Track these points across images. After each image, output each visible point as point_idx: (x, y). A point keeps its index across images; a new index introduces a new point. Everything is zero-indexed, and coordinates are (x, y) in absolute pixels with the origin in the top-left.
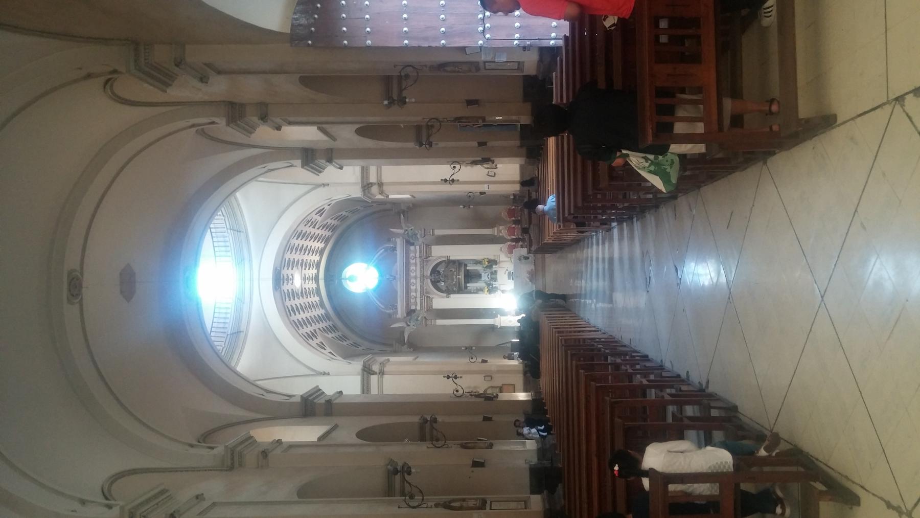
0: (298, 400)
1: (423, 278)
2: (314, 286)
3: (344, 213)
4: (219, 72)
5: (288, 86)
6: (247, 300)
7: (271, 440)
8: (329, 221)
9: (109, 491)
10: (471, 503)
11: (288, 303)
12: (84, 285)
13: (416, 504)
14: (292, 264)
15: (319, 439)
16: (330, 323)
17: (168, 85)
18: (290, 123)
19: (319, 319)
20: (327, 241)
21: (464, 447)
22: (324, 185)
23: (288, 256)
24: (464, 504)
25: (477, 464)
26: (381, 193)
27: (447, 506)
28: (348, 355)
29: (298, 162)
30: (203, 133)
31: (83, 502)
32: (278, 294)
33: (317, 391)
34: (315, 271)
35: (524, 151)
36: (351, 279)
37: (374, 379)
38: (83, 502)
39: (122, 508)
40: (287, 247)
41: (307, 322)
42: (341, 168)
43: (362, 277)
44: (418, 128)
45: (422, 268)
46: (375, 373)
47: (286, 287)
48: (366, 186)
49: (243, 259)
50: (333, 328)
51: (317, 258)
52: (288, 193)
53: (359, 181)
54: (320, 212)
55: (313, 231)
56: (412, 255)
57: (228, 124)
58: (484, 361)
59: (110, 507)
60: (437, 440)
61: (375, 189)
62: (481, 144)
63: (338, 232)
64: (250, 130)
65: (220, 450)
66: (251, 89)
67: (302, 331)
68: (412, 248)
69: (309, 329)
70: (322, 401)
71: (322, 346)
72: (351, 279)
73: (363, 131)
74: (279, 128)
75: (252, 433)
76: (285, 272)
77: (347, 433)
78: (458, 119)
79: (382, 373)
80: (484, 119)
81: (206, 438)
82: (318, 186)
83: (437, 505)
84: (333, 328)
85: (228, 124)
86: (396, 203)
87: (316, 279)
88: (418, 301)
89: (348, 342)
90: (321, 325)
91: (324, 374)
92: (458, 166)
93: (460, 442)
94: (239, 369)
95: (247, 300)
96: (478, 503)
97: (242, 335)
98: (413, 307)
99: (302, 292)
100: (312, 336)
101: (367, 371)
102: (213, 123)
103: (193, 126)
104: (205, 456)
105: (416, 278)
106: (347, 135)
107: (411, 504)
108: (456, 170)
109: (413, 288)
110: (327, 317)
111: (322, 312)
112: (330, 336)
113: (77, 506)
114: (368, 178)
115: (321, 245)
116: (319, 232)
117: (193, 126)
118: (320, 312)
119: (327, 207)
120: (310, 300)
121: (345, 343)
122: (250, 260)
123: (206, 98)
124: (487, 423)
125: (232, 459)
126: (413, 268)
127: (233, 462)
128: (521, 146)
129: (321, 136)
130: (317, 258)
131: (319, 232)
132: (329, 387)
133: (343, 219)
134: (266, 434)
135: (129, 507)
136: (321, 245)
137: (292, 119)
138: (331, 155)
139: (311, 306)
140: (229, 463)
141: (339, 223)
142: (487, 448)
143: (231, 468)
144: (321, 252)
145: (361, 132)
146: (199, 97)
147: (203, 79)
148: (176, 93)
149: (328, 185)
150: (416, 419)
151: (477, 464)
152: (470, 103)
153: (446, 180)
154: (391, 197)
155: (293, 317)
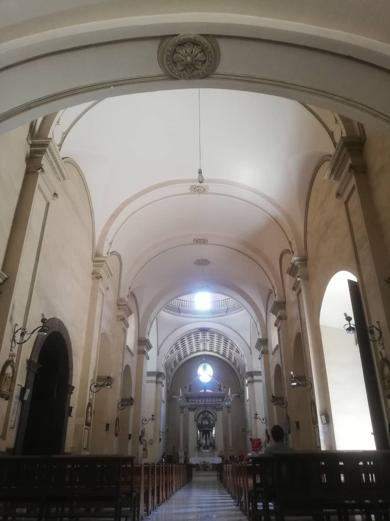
0: (147, 337)
1: (205, 406)
2: (201, 349)
3: (238, 364)
4: (298, 295)
5: (295, 328)
6: (195, 316)
7: (129, 323)
8: (233, 356)
9: (115, 254)
10: (89, 418)
11: (193, 335)
12: (202, 245)
13: (92, 388)
14: (212, 337)
15: (127, 346)
16: (183, 357)
17: (290, 274)
18: (279, 330)
19: (185, 351)
20: (224, 355)
21: (117, 420)
23: (216, 335)
24: (89, 414)
25: (108, 425)
26: (249, 382)
27: (90, 405)
28: (167, 366)
29: (261, 337)
30: (271, 292)
31: (111, 243)
32: (197, 330)
33: (150, 347)
34: (208, 349)
36: (205, 367)
37: (154, 378)
38: (111, 243)
39: (106, 257)
40: (220, 335)
41: (184, 345)
42: (260, 359)
43: (205, 374)
44: (282, 399)
45: (210, 405)
46: (157, 378)
48: (251, 374)
49: (213, 314)
50: (180, 359)
51: (215, 350)
53: (254, 370)
54: (238, 351)
55: (228, 348)
56: (217, 400)
57: (275, 302)
58: (160, 439)
59: (107, 253)
60: (122, 405)
64: (274, 312)
65: (127, 300)
66: (292, 312)
67: (179, 342)
68: (220, 400)
69: (180, 346)
70: (145, 349)
71: (172, 352)
72: (205, 367)
73: (278, 368)
74: (276, 325)
75: (133, 315)
76: (208, 334)
77: (131, 361)
78: (288, 418)
79: (157, 382)
80: (289, 432)
81: (132, 295)
82: (250, 349)
83: (90, 399)
84: (180, 359)
85: (275, 302)
86: (243, 392)
88: (193, 403)
89: (173, 366)
91: (158, 353)
92: (264, 422)
93: (119, 418)
94: (162, 312)
95: (195, 316)
96: (89, 421)
97: (178, 314)
98: (190, 400)
100: (177, 348)
101: (159, 375)
102: (275, 296)
103: (273, 287)
104: (124, 294)
105: (205, 402)
106: (275, 360)
107: (92, 386)
108: (262, 421)
109: (200, 401)
110: (186, 356)
111: (188, 353)
112: (177, 357)
113: (110, 241)
114: (256, 375)
115: (221, 352)
116: (228, 352)
117: (273, 287)
118: (188, 352)
119: (240, 354)
120: (194, 347)
121: (173, 364)
122: (213, 317)
123: (286, 292)
124: (128, 436)
125: (122, 305)
126: (210, 400)
127: (120, 304)
129: (274, 347)
130: (215, 350)
131: (228, 352)
132: (152, 353)
133: (235, 364)
134: (132, 320)
135: (107, 260)
136: (221, 353)
137: (280, 331)
138: (265, 353)
139: (191, 348)
141: (233, 361)
142: (115, 432)
143: (118, 305)
145: (278, 366)
146: (287, 289)
147: (294, 289)
148: (288, 278)
151: (108, 425)
152: (297, 424)
153: (256, 415)
155: (186, 338)
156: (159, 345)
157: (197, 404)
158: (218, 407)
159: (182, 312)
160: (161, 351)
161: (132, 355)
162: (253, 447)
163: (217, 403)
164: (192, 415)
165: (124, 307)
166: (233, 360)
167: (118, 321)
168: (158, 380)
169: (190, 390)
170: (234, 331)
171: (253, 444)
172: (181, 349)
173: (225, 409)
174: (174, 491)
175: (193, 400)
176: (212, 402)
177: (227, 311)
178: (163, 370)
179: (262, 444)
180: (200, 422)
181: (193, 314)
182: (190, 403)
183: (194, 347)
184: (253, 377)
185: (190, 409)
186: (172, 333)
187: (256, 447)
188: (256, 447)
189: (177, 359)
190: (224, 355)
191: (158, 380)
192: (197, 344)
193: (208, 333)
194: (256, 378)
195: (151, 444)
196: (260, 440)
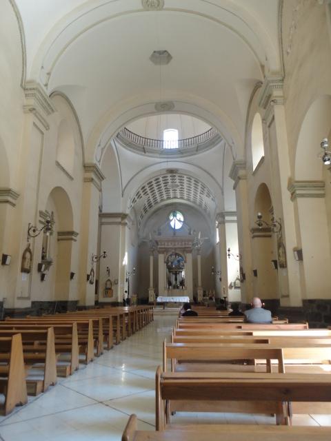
1: (175, 249)
2: (172, 196)
11: (161, 179)
19: (155, 199)
23: (185, 179)
26: (219, 223)
42: (234, 188)
47: (169, 175)
49: (182, 153)
50: (150, 206)
51: (186, 198)
61: (220, 219)
62: (255, 273)
63: (198, 208)
69: (148, 190)
87: (175, 198)
88: (163, 247)
89: (143, 213)
90: (152, 200)
97: (143, 153)
110: (156, 203)
115: (192, 200)
118: (159, 199)
122: (181, 157)
125: (30, 89)
130: (186, 198)
133: (205, 210)
139: (161, 195)
140: (27, 87)
144: (188, 200)
150: (76, 229)
154: (217, 229)
156: (124, 185)
158: (189, 249)
160: (125, 193)
161: (71, 178)
163: (187, 246)
164: (161, 258)
165: (33, 92)
166: (203, 206)
167: (25, 112)
169: (160, 234)
170: (205, 171)
172: (150, 194)
174: (138, 328)
177: (198, 149)
178: (128, 212)
180: (170, 264)
182: (159, 246)
183: (164, 193)
184: (224, 218)
185: (159, 252)
189: (147, 205)
190: (194, 202)
192: (167, 190)
193: (177, 175)
194: (227, 218)
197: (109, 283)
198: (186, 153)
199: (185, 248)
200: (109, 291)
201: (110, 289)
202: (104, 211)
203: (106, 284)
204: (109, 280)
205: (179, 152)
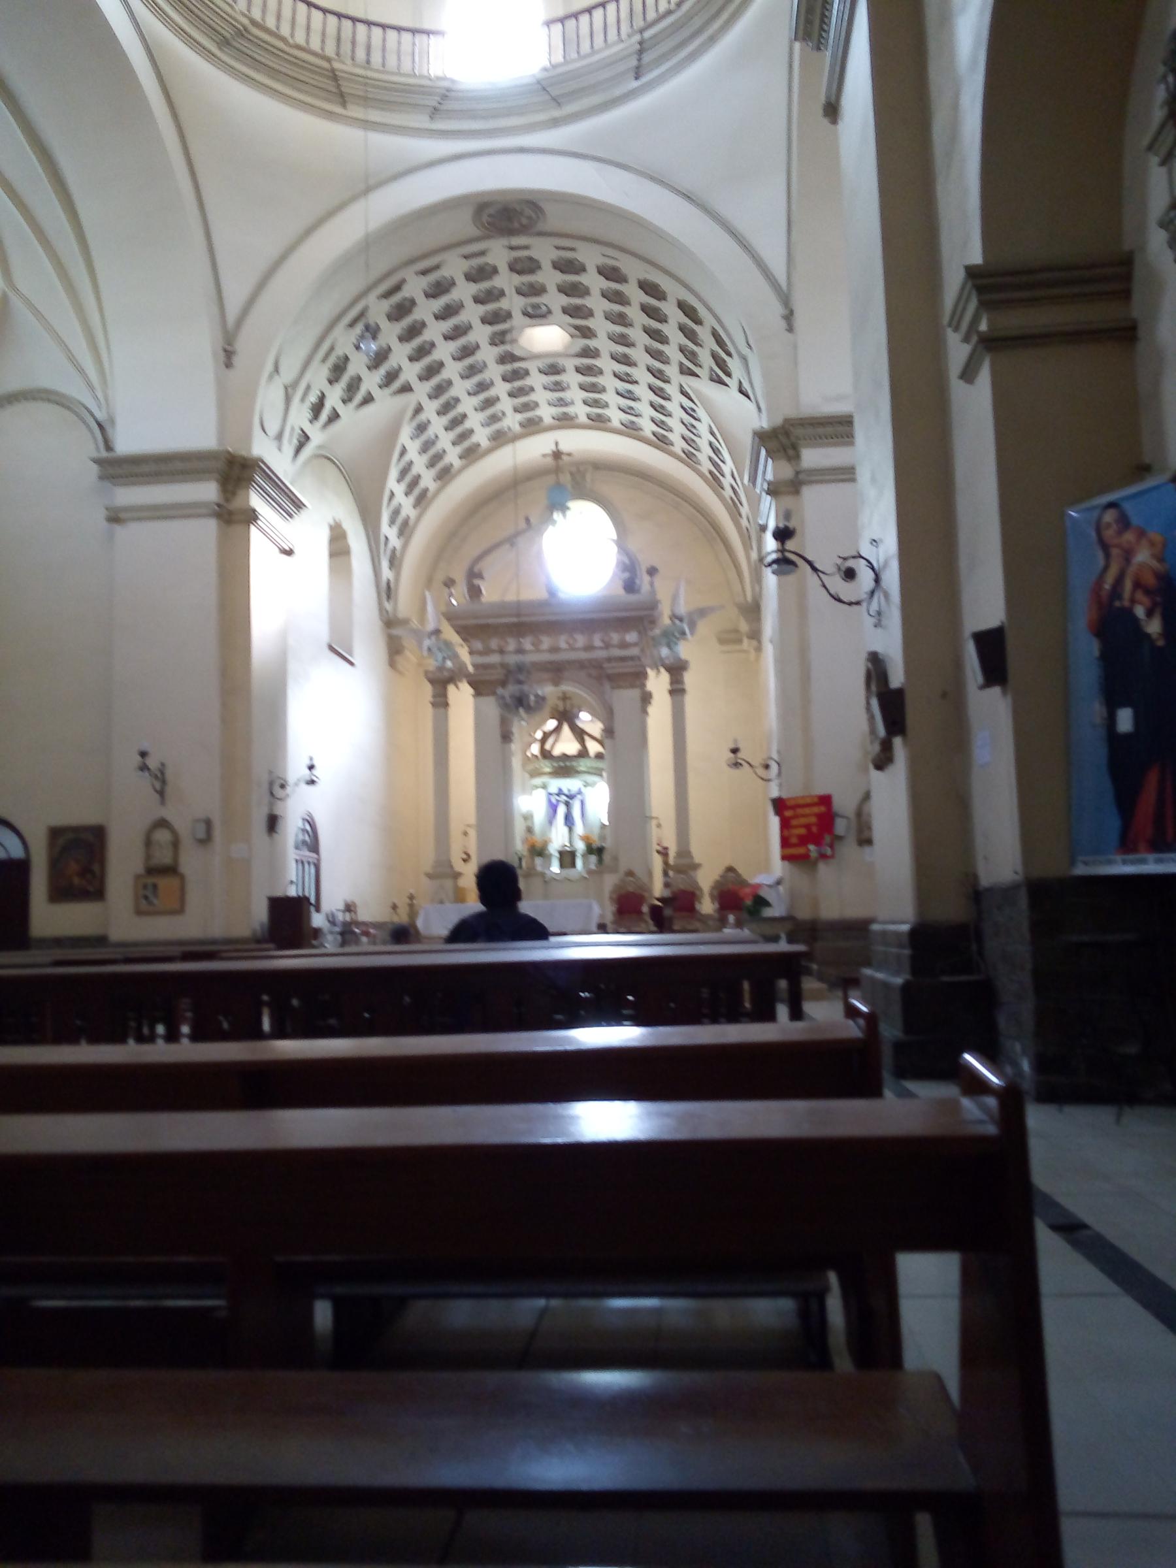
22: (789, 317)
35: (951, 909)
37: (208, 491)
45: (581, 665)
47: (498, 253)
49: (557, 101)
52: (761, 211)
56: (615, 637)
88: (494, 659)
91: (228, 356)
99: (513, 358)
108: (837, 584)
109: (527, 643)
122: (555, 123)
126: (581, 640)
128: (977, 895)
149: (790, 329)
156: (233, 309)
157: (512, 659)
158: (628, 668)
159: (366, 101)
162: (785, 842)
168: (236, 504)
171: (785, 824)
173: (658, 683)
175: (494, 643)
176: (589, 648)
179: (840, 827)
181: (435, 112)
184: (797, 457)
186: (309, 231)
187: (804, 841)
188: (804, 841)
191: (236, 504)
194: (812, 457)
195: (206, 840)
196: (826, 800)
197: (162, 836)
198: (574, 95)
199: (609, 660)
200: (165, 883)
201: (171, 870)
202: (127, 443)
203: (148, 843)
204: (162, 823)
205: (557, 96)
